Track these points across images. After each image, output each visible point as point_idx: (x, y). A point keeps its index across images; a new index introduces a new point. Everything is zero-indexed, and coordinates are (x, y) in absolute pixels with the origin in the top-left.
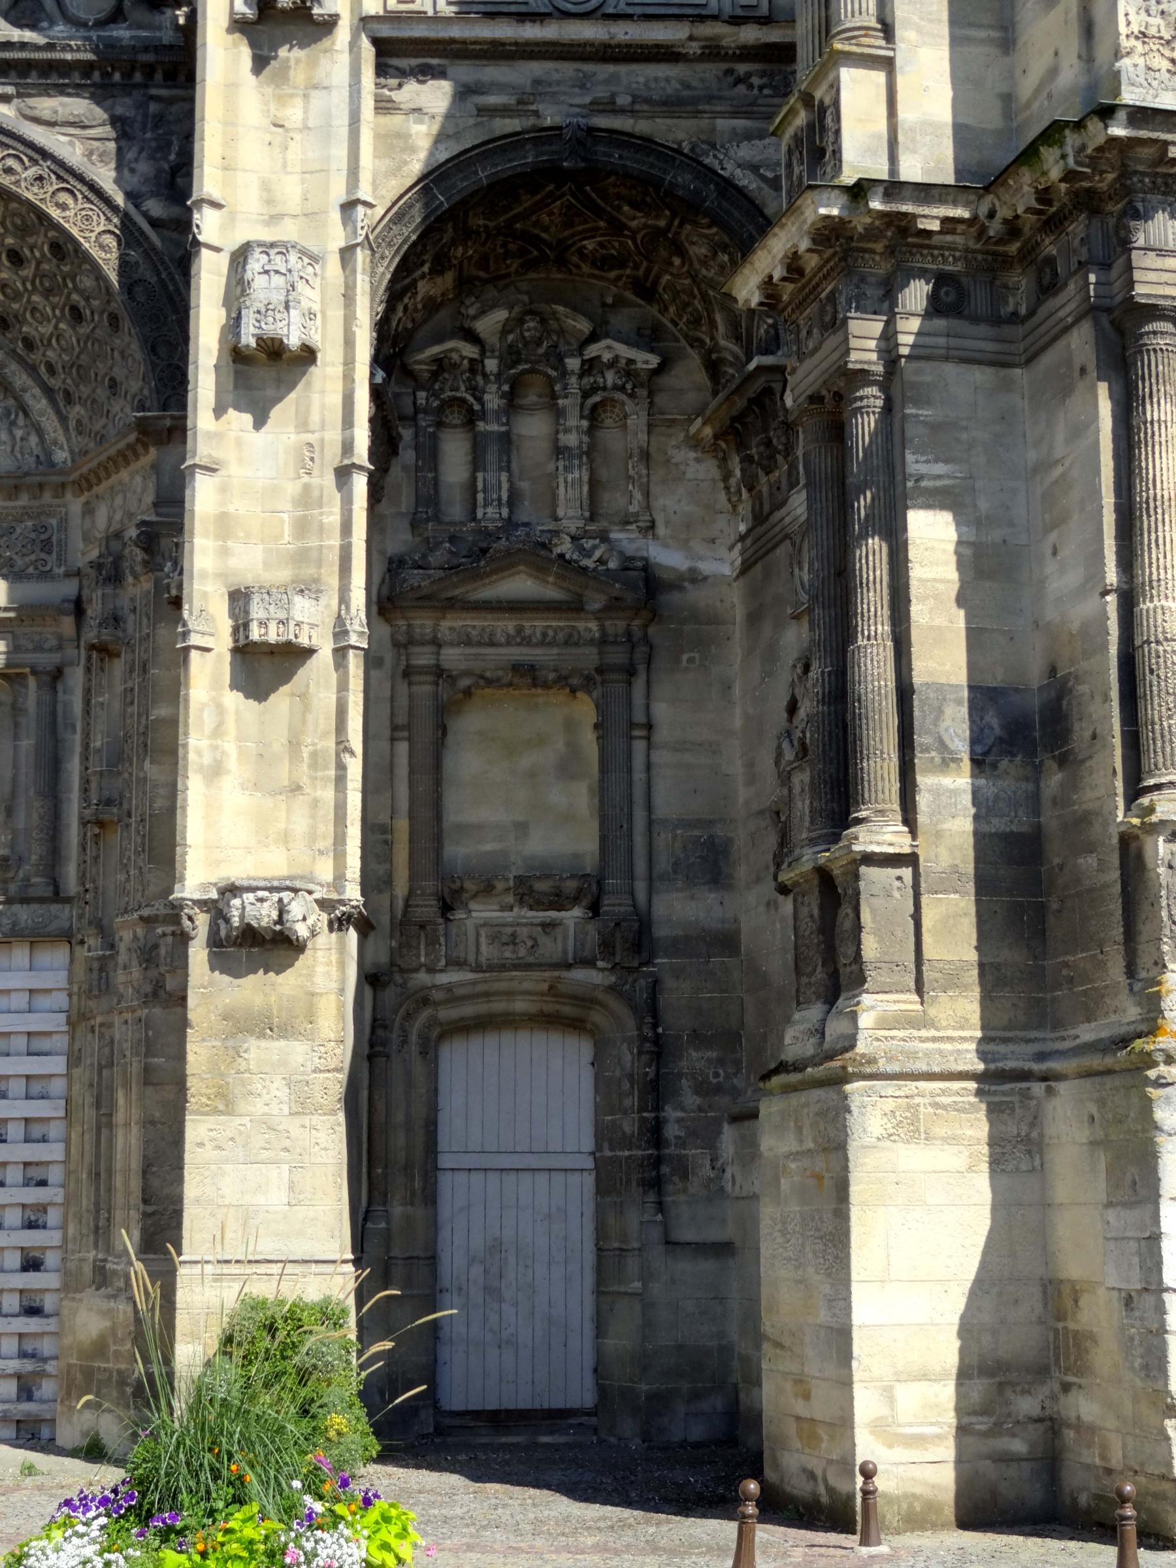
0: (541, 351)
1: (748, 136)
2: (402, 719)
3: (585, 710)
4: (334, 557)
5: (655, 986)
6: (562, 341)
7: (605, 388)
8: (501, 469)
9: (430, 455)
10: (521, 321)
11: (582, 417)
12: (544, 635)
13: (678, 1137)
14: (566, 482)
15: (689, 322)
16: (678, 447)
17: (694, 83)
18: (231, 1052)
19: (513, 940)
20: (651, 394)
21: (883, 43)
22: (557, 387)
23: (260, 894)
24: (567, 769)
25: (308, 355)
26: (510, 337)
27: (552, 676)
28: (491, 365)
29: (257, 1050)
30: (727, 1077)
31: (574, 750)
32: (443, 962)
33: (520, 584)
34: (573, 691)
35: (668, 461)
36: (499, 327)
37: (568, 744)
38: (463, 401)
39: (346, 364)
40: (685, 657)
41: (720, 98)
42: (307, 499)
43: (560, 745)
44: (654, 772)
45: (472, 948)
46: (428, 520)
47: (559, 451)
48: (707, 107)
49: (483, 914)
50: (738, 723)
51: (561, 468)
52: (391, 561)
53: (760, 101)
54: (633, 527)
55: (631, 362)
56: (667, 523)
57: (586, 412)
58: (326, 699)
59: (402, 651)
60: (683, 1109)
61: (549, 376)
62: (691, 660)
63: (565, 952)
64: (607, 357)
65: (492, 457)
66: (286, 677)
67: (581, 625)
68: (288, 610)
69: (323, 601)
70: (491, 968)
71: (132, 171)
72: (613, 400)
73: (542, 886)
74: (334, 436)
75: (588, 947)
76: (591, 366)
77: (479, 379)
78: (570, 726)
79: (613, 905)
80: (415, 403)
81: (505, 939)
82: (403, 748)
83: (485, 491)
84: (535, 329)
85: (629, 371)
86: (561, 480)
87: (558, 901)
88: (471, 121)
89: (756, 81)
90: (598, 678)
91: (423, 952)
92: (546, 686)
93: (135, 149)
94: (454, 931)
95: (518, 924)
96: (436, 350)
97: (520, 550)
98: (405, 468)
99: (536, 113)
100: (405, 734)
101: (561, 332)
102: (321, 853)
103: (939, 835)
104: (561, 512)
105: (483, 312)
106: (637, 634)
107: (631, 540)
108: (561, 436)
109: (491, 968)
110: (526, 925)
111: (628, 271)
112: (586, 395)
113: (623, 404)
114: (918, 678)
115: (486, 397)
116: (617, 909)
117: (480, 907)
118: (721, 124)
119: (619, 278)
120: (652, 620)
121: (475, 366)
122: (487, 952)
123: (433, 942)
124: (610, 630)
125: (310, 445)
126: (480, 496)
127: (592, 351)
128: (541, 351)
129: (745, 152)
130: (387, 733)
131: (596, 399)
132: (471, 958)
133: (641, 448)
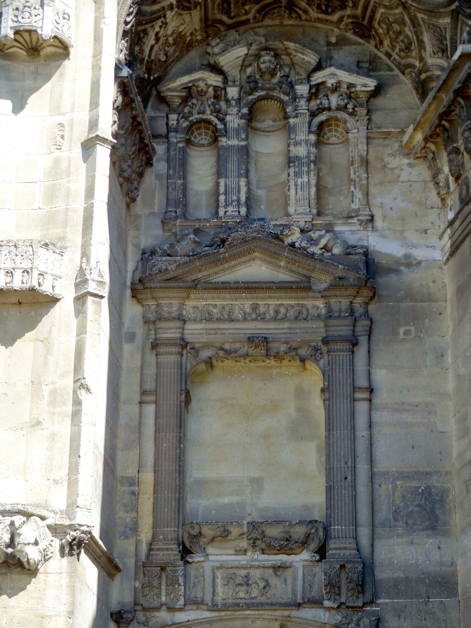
0: (275, 80)
2: (150, 385)
3: (314, 378)
4: (78, 218)
6: (293, 72)
7: (329, 109)
8: (240, 176)
9: (181, 167)
10: (258, 56)
11: (310, 132)
12: (277, 312)
14: (296, 185)
15: (401, 50)
16: (393, 155)
20: (369, 112)
22: (289, 109)
24: (297, 432)
25: (62, 49)
26: (249, 70)
27: (283, 348)
28: (233, 92)
31: (304, 413)
32: (182, 602)
33: (256, 269)
34: (303, 360)
35: (385, 166)
36: (240, 61)
37: (298, 410)
38: (209, 122)
39: (94, 56)
40: (402, 330)
42: (56, 171)
43: (291, 409)
44: (375, 430)
45: (209, 588)
46: (177, 218)
47: (290, 161)
49: (220, 558)
50: (450, 386)
51: (292, 174)
52: (144, 253)
54: (355, 220)
55: (350, 86)
56: (385, 217)
57: (314, 128)
58: (66, 343)
59: (152, 326)
61: (281, 101)
62: (407, 333)
63: (294, 592)
64: (330, 82)
65: (232, 165)
66: (32, 324)
67: (309, 303)
68: (32, 261)
69: (67, 255)
70: (226, 607)
72: (337, 119)
74: (83, 117)
76: (316, 91)
77: (223, 105)
78: (300, 394)
79: (338, 548)
80: (167, 124)
81: (239, 580)
82: (150, 410)
83: (226, 193)
84: (270, 61)
85: (351, 94)
86: (292, 183)
87: (287, 545)
90: (325, 349)
91: (164, 592)
92: (278, 357)
95: (252, 567)
96: (185, 79)
97: (254, 238)
98: (158, 177)
100: (153, 398)
101: (293, 65)
102: (56, 482)
104: (291, 210)
105: (224, 51)
106: (359, 310)
107: (353, 232)
108: (292, 148)
109: (226, 607)
110: (259, 567)
111: (348, 11)
112: (313, 115)
113: (345, 122)
115: (228, 118)
116: (342, 552)
117: (217, 552)
119: (341, 19)
120: (372, 298)
121: (219, 92)
123: (173, 582)
124: (335, 307)
125: (61, 125)
126: (222, 198)
127: (318, 77)
128: (275, 80)
130: (137, 398)
131: (322, 117)
133: (361, 157)
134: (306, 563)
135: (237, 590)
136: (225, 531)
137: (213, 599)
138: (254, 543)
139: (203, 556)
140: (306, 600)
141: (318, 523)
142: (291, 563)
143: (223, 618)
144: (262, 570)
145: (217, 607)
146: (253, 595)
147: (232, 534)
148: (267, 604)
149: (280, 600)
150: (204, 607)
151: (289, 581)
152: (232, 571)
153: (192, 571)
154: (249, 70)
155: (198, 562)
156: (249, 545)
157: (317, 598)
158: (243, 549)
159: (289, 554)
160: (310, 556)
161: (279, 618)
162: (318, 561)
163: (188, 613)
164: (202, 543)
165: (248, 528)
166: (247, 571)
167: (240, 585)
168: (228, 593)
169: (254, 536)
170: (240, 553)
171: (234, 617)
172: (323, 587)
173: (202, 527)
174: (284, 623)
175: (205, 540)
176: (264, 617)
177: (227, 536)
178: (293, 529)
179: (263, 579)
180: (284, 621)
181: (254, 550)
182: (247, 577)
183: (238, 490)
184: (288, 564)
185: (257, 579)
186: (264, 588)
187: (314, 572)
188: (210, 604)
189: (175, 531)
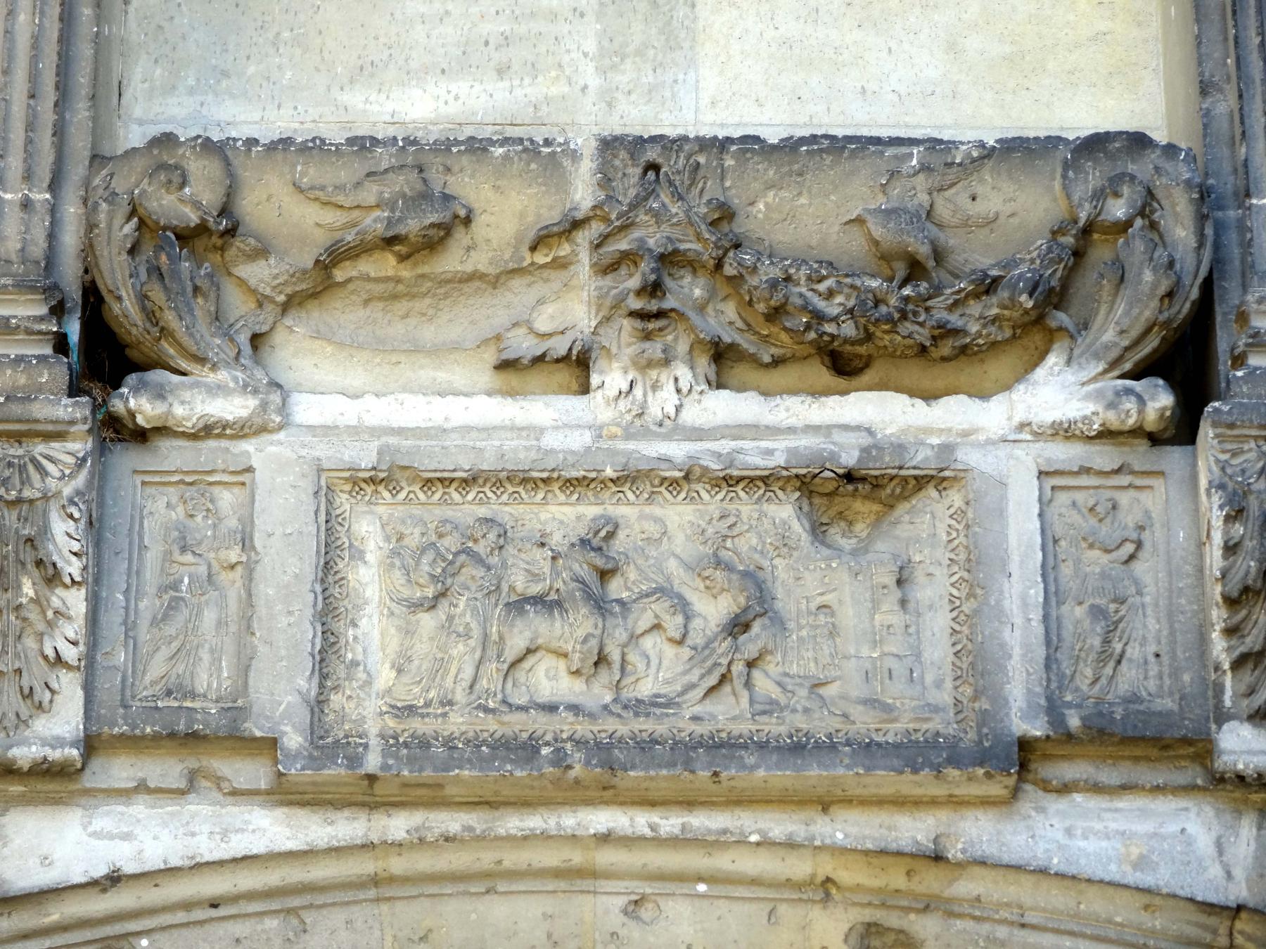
19: (598, 569)
45: (287, 627)
63: (976, 663)
73: (801, 221)
75: (1147, 631)
87: (911, 309)
94: (160, 511)
109: (414, 773)
110: (686, 479)
122: (395, 660)
132: (279, 699)
134: (1063, 453)
135: (517, 642)
136: (424, 196)
137: (318, 705)
138: (654, 289)
139: (247, 388)
140: (1074, 722)
141: (1154, 156)
142: (947, 449)
143: (397, 865)
144: (713, 502)
145: (354, 761)
146: (646, 689)
147: (480, 222)
148: (762, 746)
149: (864, 723)
150: (249, 772)
151: (934, 589)
152: (467, 508)
153: (153, 506)
155: (207, 431)
156: (610, 311)
157: (1168, 704)
158: (560, 347)
159: (929, 396)
160: (1099, 395)
161: (847, 875)
162: (1155, 439)
163: (107, 818)
164: (237, 304)
165: (606, 180)
166: (591, 511)
167: (546, 603)
168: (440, 666)
169: (653, 237)
170: (535, 378)
171: (486, 859)
172: (1218, 616)
173: (246, 175)
174: (893, 920)
175: (259, 273)
176: (724, 862)
177: (434, 241)
178: (959, 195)
179: (719, 563)
180: (887, 898)
181: (655, 349)
182: (599, 557)
183: (507, 40)
184: (921, 459)
185: (672, 565)
186: (738, 626)
187: (1129, 518)
188: (293, 740)
189: (26, 205)
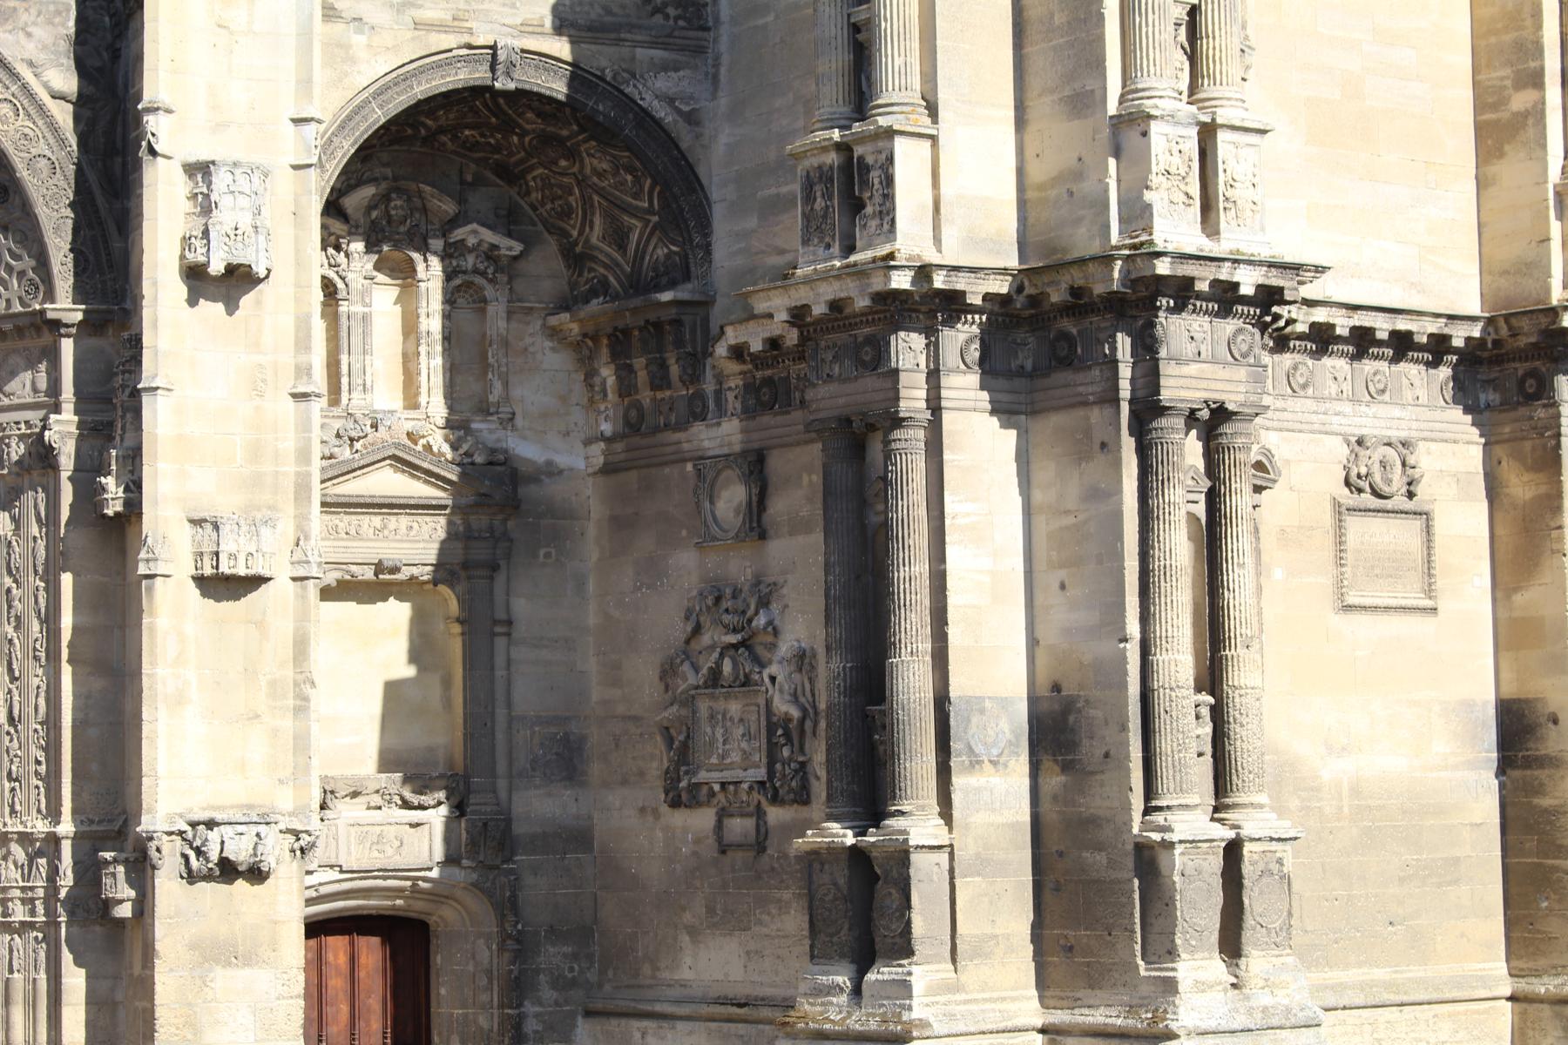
0: (402, 229)
1: (665, 67)
5: (515, 887)
13: (536, 1032)
17: (616, 10)
18: (198, 982)
20: (511, 279)
21: (928, 121)
23: (240, 828)
26: (374, 214)
29: (224, 979)
30: (582, 972)
39: (298, 285)
40: (542, 552)
41: (640, 27)
48: (628, 36)
50: (592, 620)
53: (676, 33)
54: (494, 418)
55: (495, 247)
58: (283, 629)
60: (541, 1004)
62: (548, 555)
64: (471, 241)
71: (29, 35)
74: (288, 359)
88: (409, 35)
89: (671, 11)
90: (463, 574)
93: (33, 11)
99: (470, 31)
101: (425, 210)
103: (967, 827)
107: (491, 431)
114: (954, 693)
118: (640, 53)
127: (458, 234)
129: (663, 83)
154: (374, 214)
